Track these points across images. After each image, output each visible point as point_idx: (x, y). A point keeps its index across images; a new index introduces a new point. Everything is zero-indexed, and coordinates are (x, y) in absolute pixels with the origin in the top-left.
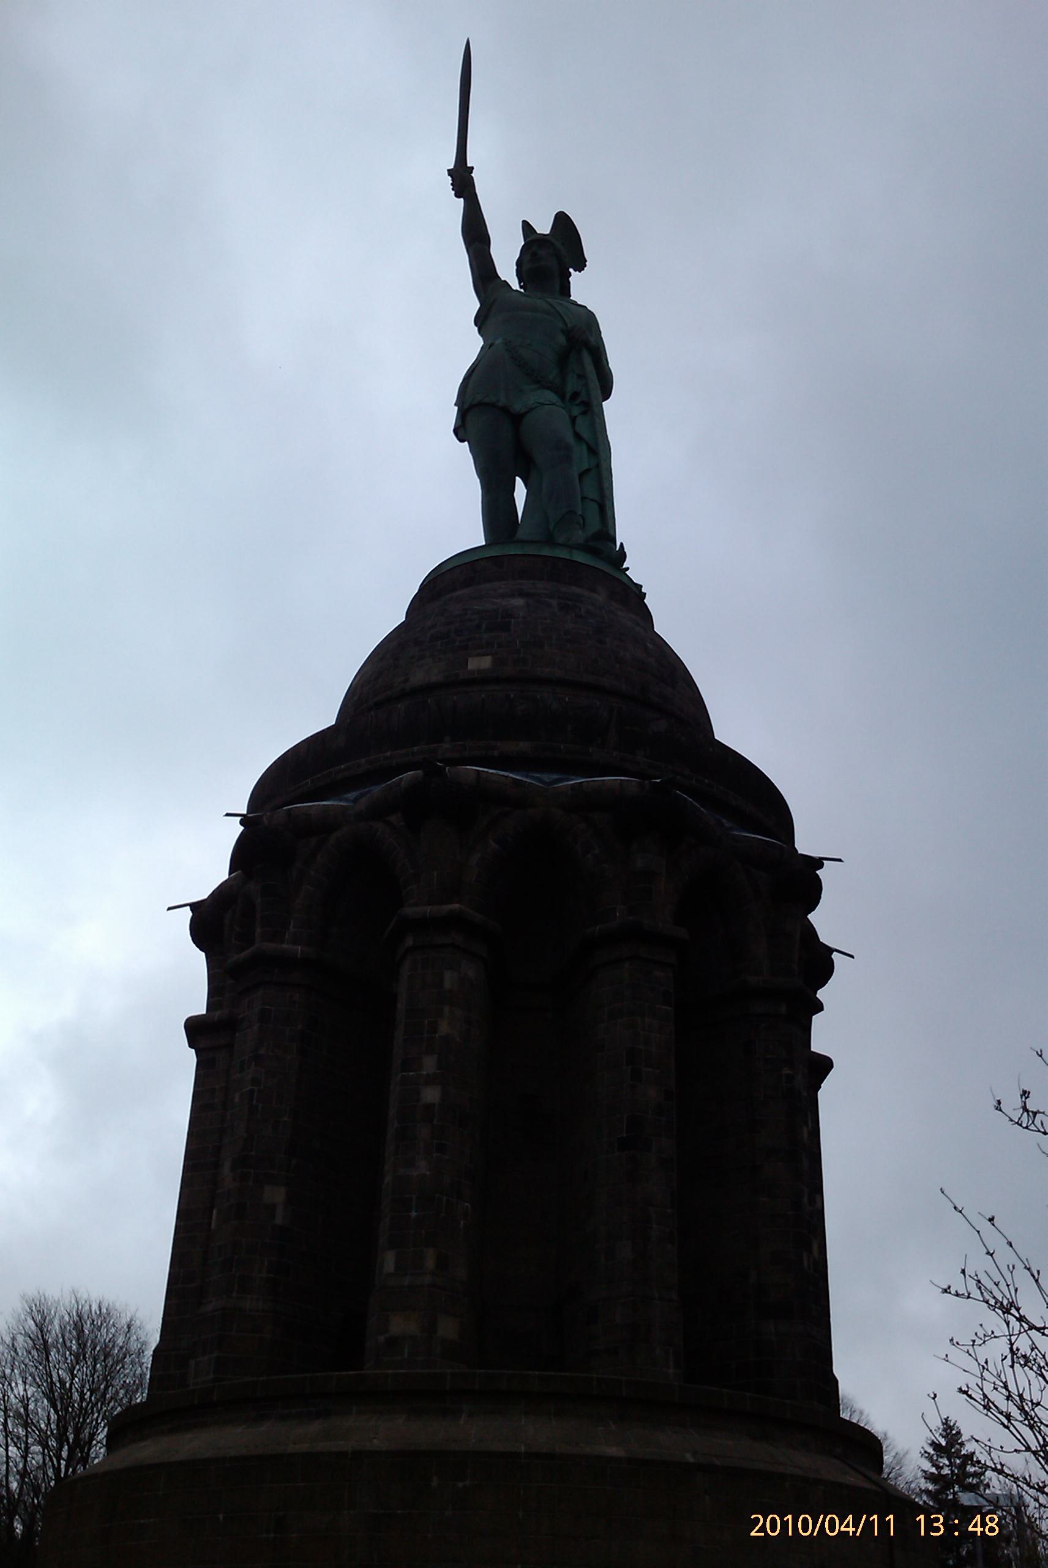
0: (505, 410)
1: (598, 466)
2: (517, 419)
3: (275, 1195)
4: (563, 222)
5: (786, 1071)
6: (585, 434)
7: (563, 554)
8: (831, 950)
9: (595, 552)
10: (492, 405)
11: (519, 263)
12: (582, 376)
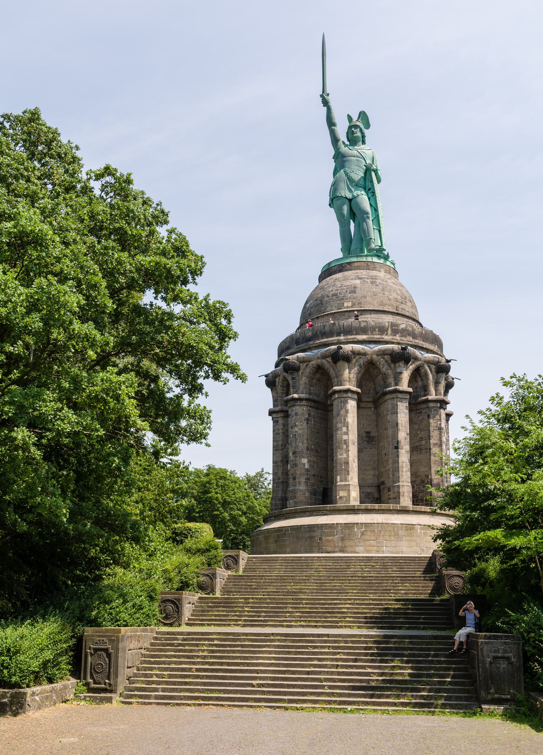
0: (346, 198)
1: (378, 216)
2: (350, 200)
3: (305, 461)
4: (363, 115)
5: (439, 423)
6: (373, 204)
7: (369, 259)
8: (453, 379)
9: (379, 257)
10: (342, 197)
11: (347, 133)
12: (372, 181)
